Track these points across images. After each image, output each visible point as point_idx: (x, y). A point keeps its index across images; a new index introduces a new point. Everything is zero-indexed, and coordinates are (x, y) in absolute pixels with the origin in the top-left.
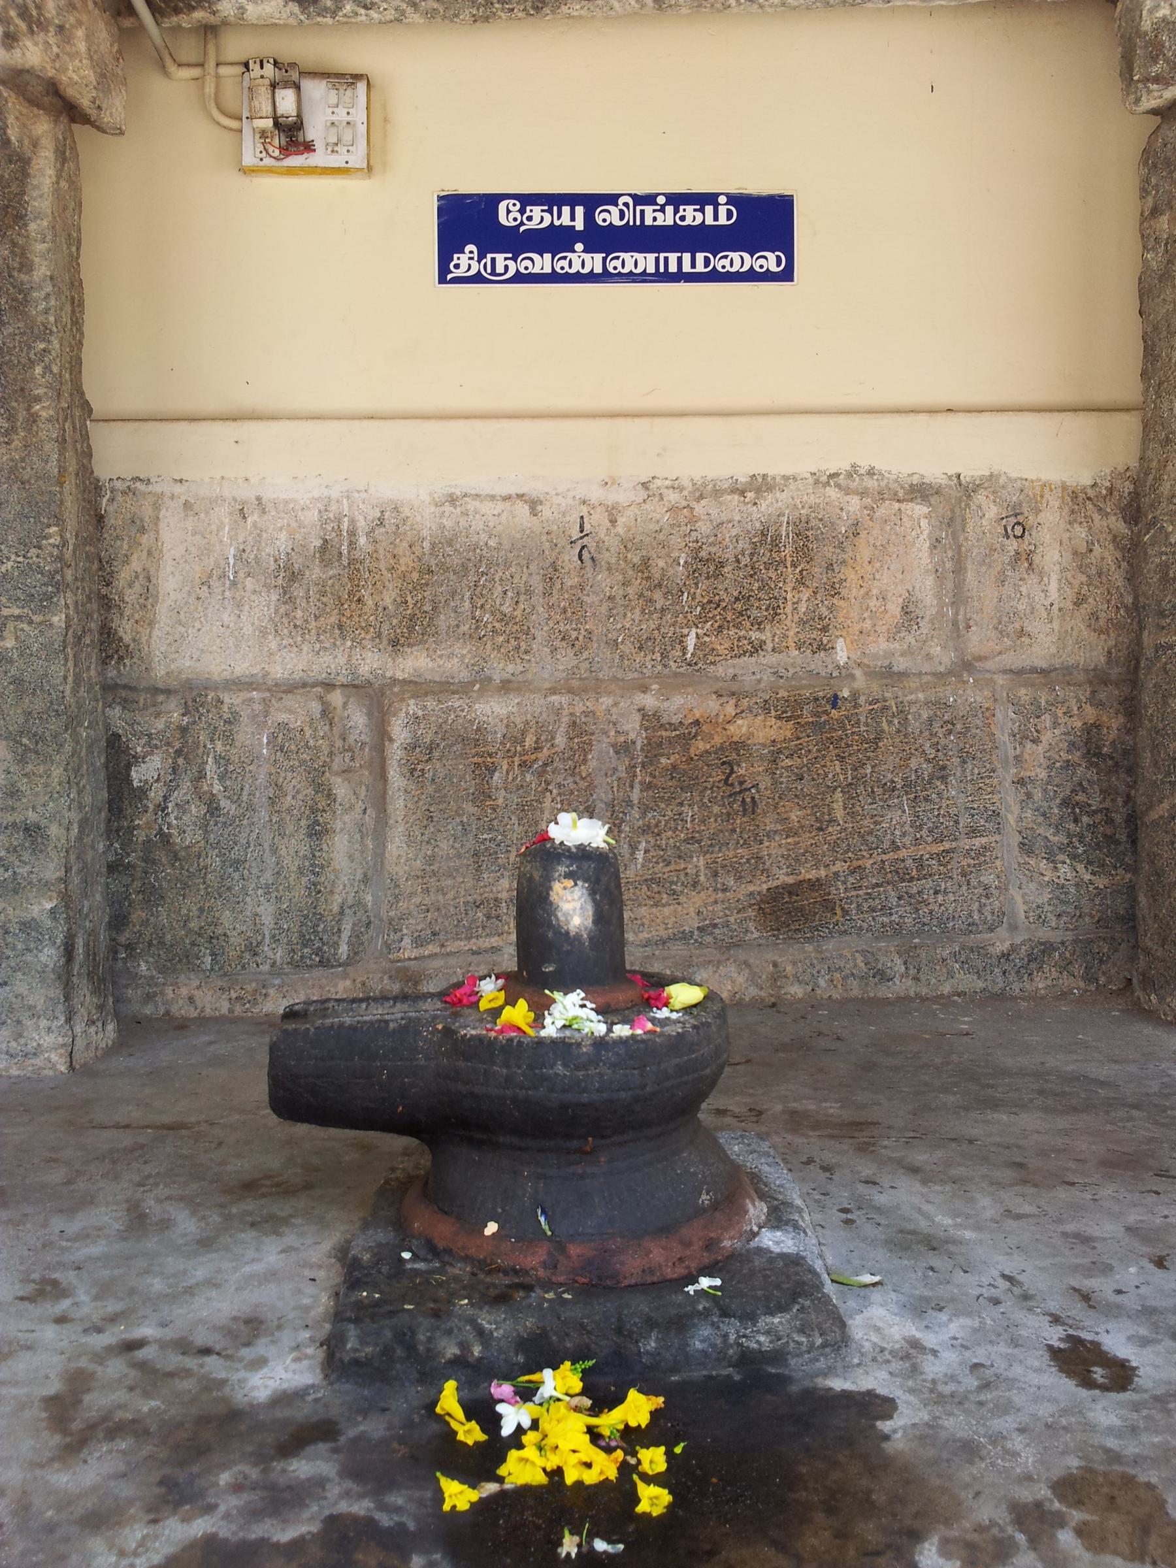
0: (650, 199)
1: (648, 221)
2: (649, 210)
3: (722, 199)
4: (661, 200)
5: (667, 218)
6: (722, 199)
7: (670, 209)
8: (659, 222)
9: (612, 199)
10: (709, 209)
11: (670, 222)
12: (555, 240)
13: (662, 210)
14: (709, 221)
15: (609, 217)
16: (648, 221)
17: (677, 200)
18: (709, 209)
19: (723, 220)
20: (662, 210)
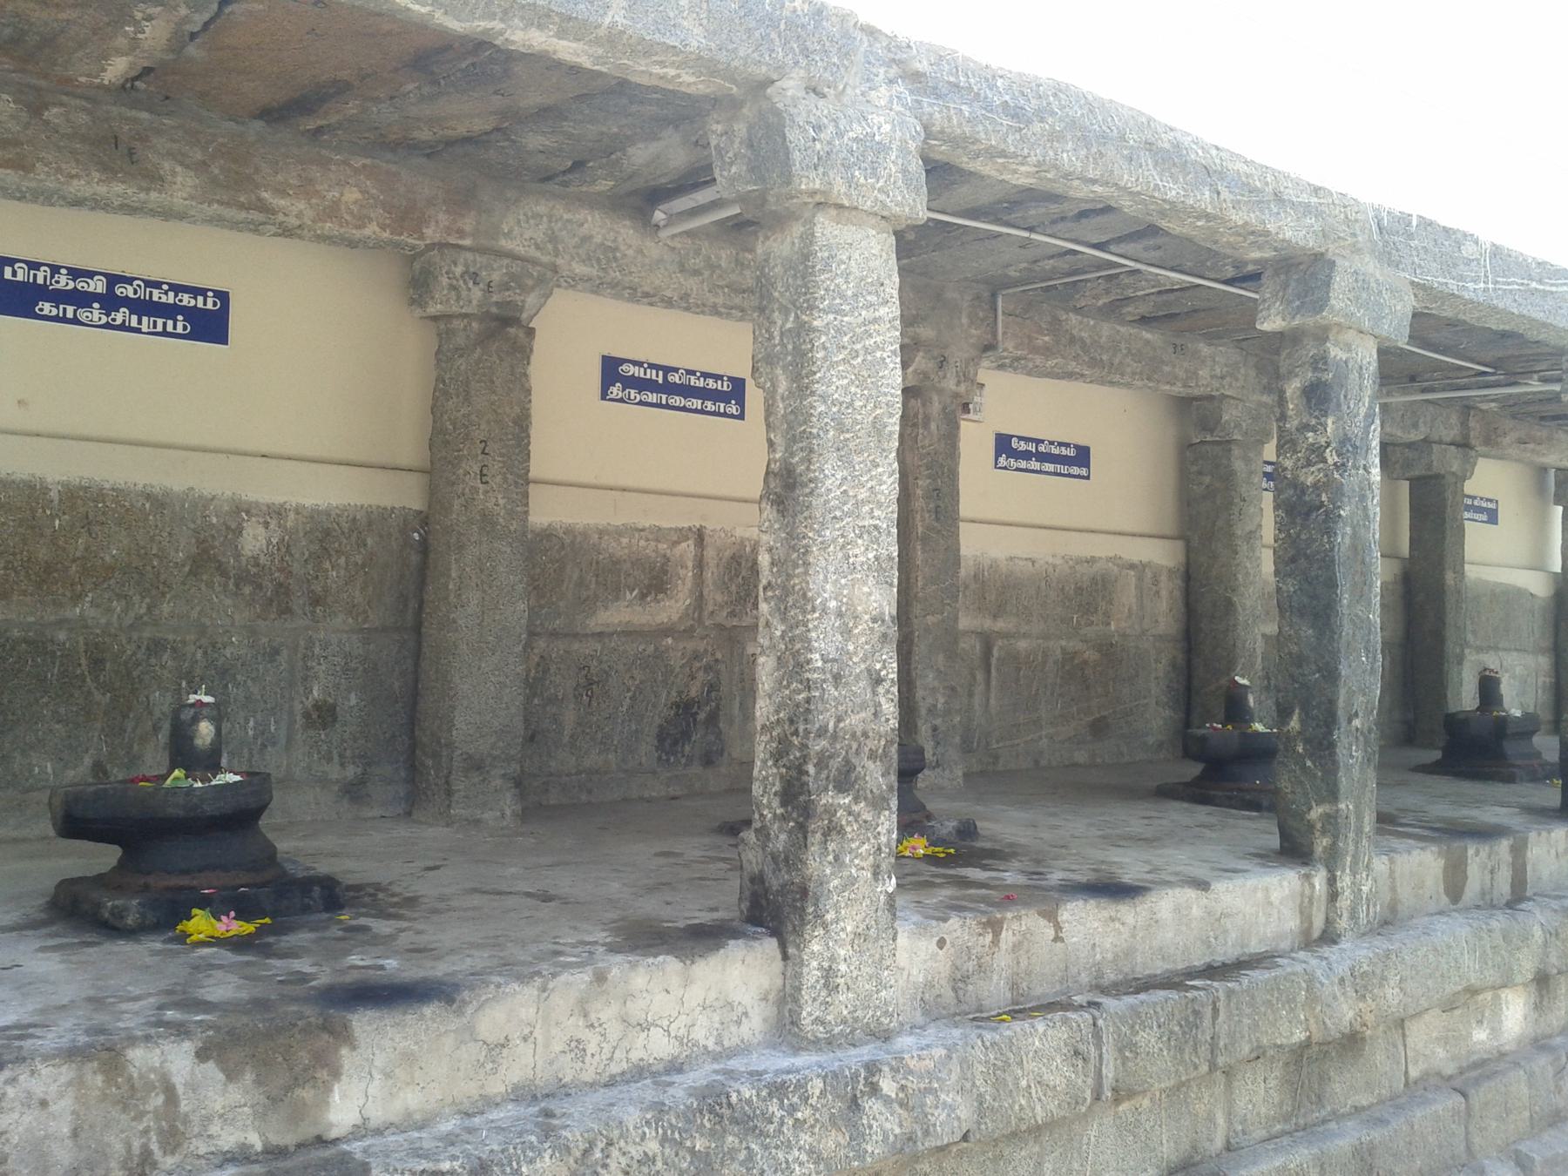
0: (157, 285)
1: (155, 298)
2: (156, 293)
3: (210, 294)
4: (165, 287)
5: (170, 298)
6: (210, 294)
7: (171, 294)
8: (164, 300)
9: (130, 281)
10: (200, 299)
11: (171, 301)
12: (82, 299)
13: (166, 293)
14: (200, 305)
15: (129, 291)
16: (155, 298)
17: (177, 289)
18: (200, 299)
19: (210, 306)
20: (166, 293)
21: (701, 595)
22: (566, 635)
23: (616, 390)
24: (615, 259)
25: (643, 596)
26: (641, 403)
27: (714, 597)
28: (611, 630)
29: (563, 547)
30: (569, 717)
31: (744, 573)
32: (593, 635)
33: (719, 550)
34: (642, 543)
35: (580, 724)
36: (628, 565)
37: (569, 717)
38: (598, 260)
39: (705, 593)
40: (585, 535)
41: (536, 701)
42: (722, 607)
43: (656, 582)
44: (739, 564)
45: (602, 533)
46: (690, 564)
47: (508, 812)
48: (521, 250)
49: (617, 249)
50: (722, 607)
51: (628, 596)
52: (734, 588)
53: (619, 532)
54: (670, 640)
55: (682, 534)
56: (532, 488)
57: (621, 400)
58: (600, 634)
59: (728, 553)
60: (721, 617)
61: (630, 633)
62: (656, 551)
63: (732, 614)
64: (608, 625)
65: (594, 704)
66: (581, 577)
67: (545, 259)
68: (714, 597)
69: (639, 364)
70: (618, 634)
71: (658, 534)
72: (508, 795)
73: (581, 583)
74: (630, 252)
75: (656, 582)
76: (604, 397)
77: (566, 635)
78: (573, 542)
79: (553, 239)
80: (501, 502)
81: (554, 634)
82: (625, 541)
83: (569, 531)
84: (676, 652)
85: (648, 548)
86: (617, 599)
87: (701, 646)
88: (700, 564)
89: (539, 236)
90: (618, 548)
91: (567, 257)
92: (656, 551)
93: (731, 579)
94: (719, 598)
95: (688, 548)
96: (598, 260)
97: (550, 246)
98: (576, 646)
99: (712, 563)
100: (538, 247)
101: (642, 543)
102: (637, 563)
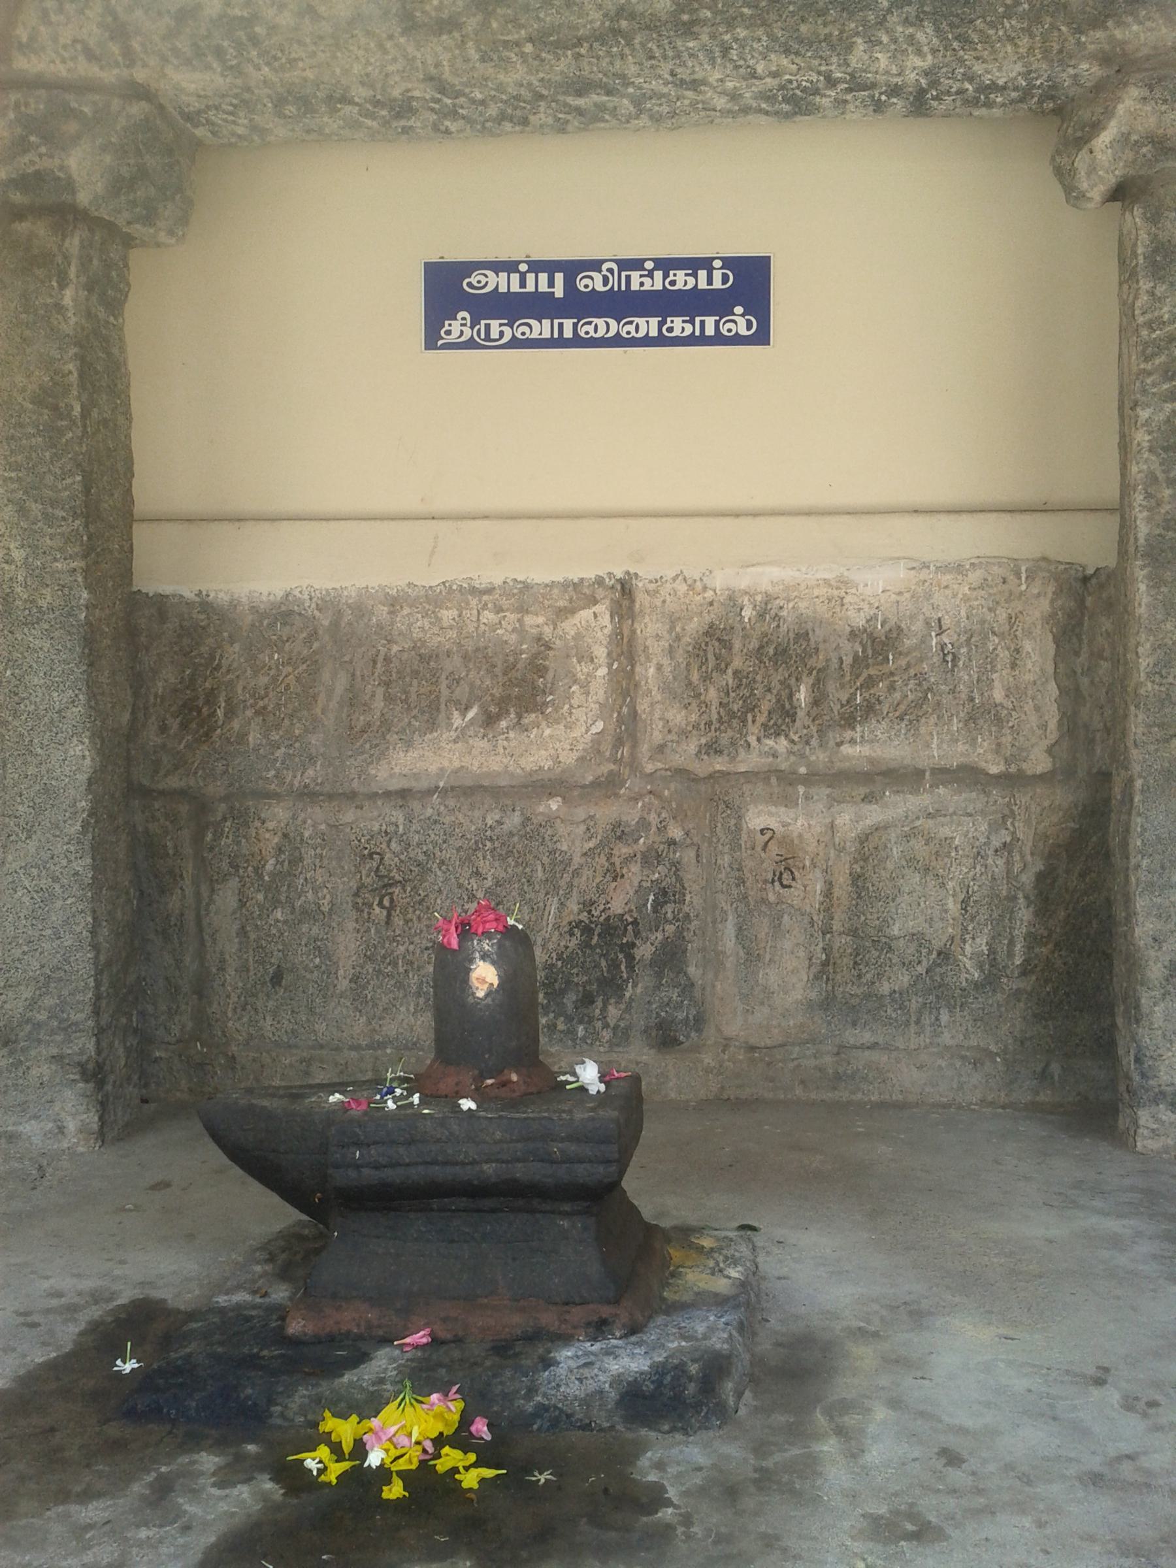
21: (634, 714)
22: (331, 797)
23: (458, 327)
24: (254, 40)
25: (489, 720)
26: (515, 343)
27: (662, 715)
28: (424, 784)
29: (313, 635)
30: (347, 945)
31: (737, 663)
32: (388, 794)
33: (673, 621)
34: (488, 616)
35: (369, 958)
36: (457, 660)
37: (347, 945)
38: (219, 53)
39: (643, 706)
40: (360, 609)
41: (279, 914)
42: (684, 734)
43: (520, 687)
44: (726, 645)
45: (394, 602)
46: (601, 652)
47: (71, 1126)
48: (61, 70)
49: (254, 18)
50: (684, 734)
51: (457, 721)
52: (712, 694)
53: (433, 600)
54: (554, 805)
55: (581, 594)
56: (135, 526)
57: (471, 344)
58: (404, 794)
59: (695, 626)
60: (686, 753)
61: (470, 791)
62: (520, 630)
63: (713, 748)
64: (416, 776)
65: (398, 921)
66: (351, 688)
67: (109, 76)
68: (662, 715)
69: (498, 267)
70: (444, 792)
71: (523, 596)
72: (68, 1093)
73: (353, 700)
74: (286, 20)
75: (520, 687)
76: (432, 340)
77: (331, 797)
78: (335, 624)
79: (119, 31)
80: (18, 555)
81: (308, 795)
82: (448, 615)
83: (329, 603)
84: (573, 829)
85: (502, 628)
86: (432, 725)
87: (632, 815)
88: (625, 649)
89: (92, 32)
90: (437, 631)
91: (153, 61)
92: (520, 630)
93: (706, 678)
94: (677, 717)
95: (595, 622)
96: (219, 53)
97: (115, 48)
98: (349, 816)
99: (657, 649)
100: (91, 56)
101: (488, 616)
102: (480, 656)
